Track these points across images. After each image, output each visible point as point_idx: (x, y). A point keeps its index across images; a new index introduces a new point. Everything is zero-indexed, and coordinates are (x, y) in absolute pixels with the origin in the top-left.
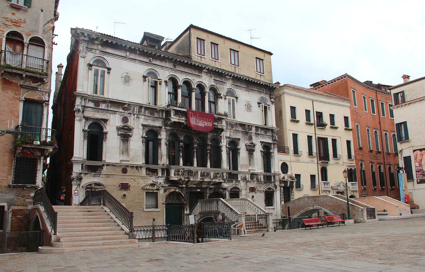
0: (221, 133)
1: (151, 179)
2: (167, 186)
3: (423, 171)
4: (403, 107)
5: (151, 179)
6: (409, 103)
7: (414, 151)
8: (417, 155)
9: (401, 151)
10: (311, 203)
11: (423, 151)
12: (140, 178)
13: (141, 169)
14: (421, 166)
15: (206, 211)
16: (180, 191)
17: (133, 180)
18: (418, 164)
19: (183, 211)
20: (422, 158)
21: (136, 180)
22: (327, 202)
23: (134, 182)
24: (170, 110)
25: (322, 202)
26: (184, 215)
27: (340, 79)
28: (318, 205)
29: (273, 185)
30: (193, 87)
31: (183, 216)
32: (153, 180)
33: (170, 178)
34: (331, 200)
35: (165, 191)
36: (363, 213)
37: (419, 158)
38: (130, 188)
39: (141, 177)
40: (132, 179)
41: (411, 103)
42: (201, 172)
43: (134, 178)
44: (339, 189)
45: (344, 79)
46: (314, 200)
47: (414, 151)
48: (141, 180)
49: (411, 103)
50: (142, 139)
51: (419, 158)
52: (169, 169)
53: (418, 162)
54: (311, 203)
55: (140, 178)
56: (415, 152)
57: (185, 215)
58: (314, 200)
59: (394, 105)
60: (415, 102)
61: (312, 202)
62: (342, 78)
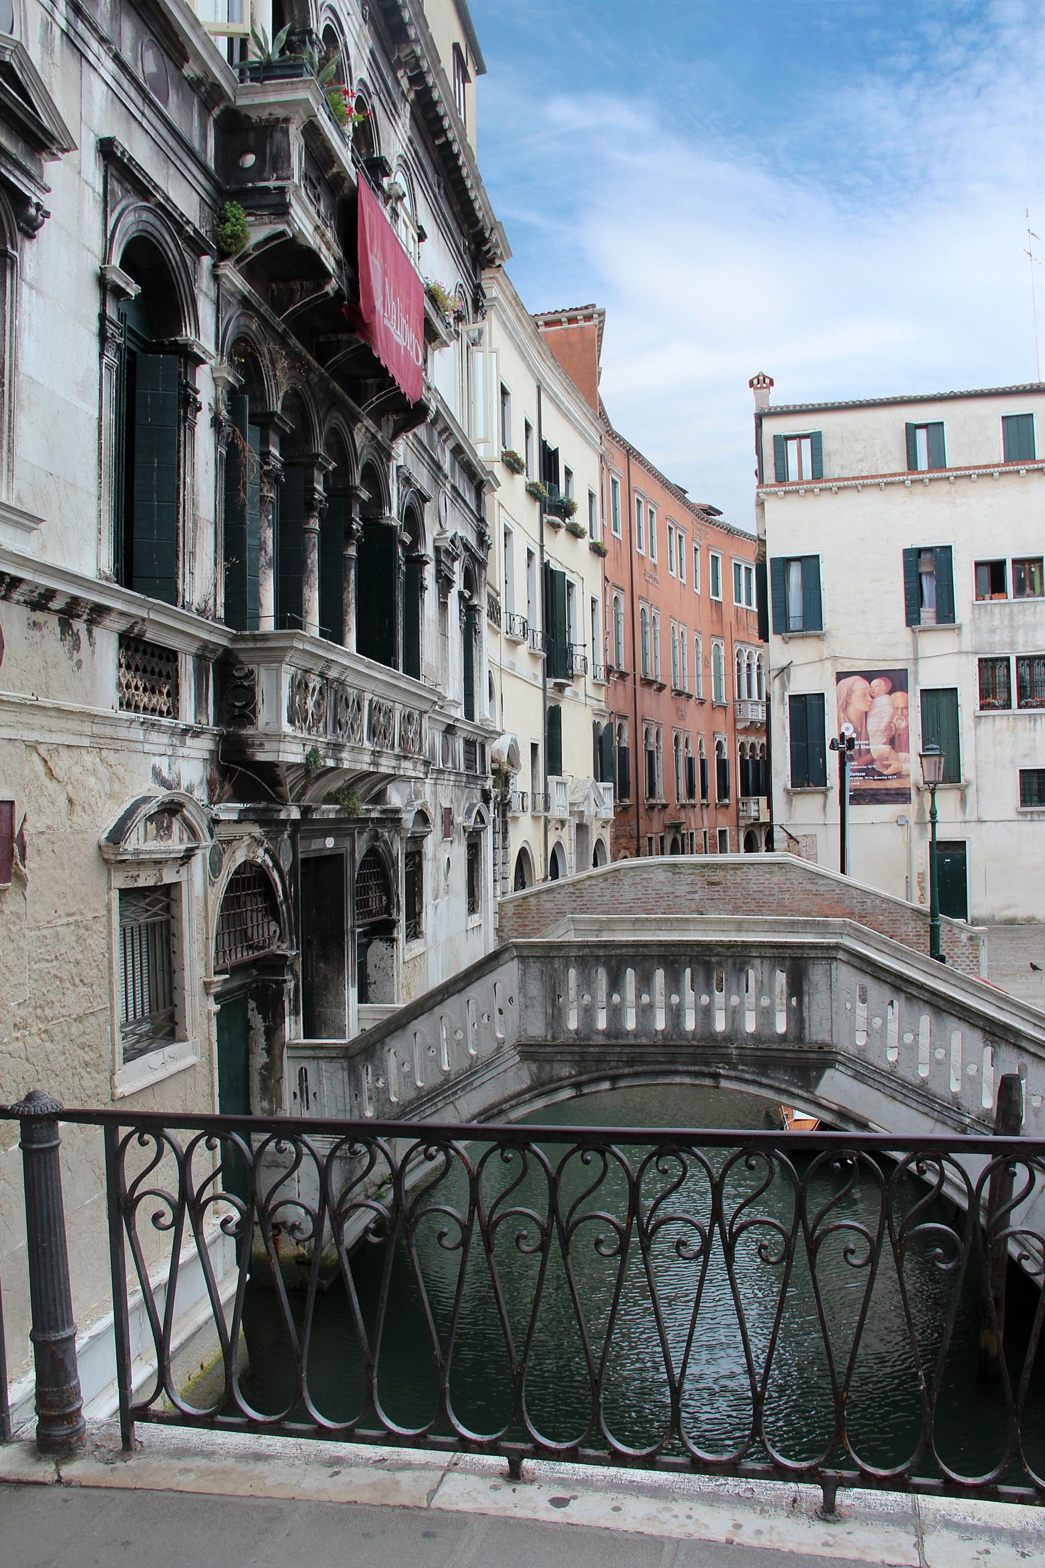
0: (395, 436)
1: (147, 747)
2: (235, 817)
3: (867, 758)
4: (810, 498)
5: (147, 747)
6: (841, 484)
7: (840, 676)
8: (849, 695)
9: (783, 670)
10: (690, 897)
11: (875, 682)
12: (86, 742)
13: (90, 632)
14: (863, 736)
15: (615, 1031)
16: (272, 857)
17: (40, 767)
18: (852, 729)
19: (258, 1022)
20: (870, 707)
21: (62, 763)
22: (787, 896)
23: (47, 781)
24: (280, 113)
25: (755, 896)
26: (269, 1050)
27: (559, 322)
28: (730, 907)
29: (478, 793)
30: (313, 25)
31: (259, 1059)
32: (158, 761)
33: (268, 746)
34: (809, 887)
35: (215, 868)
36: (978, 950)
37: (857, 705)
38: (23, 857)
39: (97, 729)
40: (33, 747)
41: (845, 488)
42: (371, 701)
43: (47, 738)
44: (586, 813)
45: (582, 328)
46: (712, 884)
47: (840, 676)
48: (89, 759)
49: (845, 488)
50: (96, 310)
51: (857, 705)
52: (242, 657)
53: (851, 722)
54: (690, 897)
55: (86, 742)
56: (846, 682)
57: (286, 1053)
58: (712, 884)
59: (773, 481)
60: (863, 486)
61: (695, 892)
62: (571, 320)
